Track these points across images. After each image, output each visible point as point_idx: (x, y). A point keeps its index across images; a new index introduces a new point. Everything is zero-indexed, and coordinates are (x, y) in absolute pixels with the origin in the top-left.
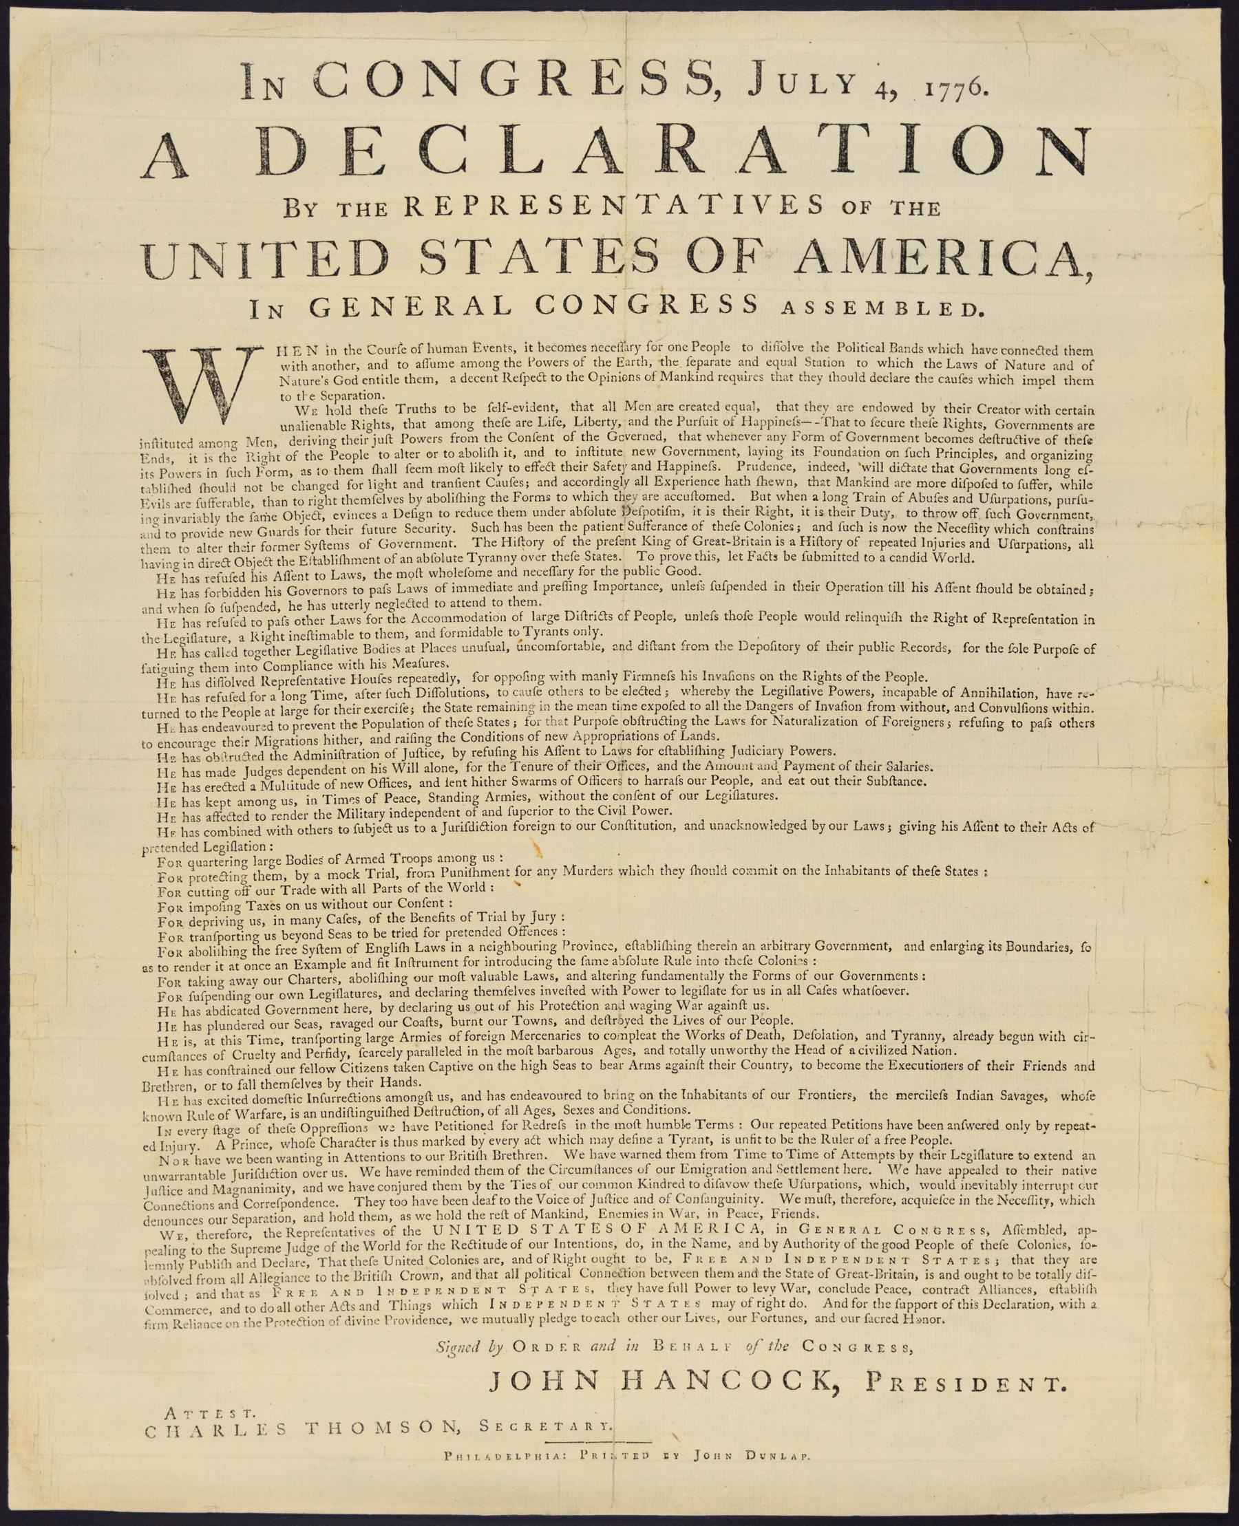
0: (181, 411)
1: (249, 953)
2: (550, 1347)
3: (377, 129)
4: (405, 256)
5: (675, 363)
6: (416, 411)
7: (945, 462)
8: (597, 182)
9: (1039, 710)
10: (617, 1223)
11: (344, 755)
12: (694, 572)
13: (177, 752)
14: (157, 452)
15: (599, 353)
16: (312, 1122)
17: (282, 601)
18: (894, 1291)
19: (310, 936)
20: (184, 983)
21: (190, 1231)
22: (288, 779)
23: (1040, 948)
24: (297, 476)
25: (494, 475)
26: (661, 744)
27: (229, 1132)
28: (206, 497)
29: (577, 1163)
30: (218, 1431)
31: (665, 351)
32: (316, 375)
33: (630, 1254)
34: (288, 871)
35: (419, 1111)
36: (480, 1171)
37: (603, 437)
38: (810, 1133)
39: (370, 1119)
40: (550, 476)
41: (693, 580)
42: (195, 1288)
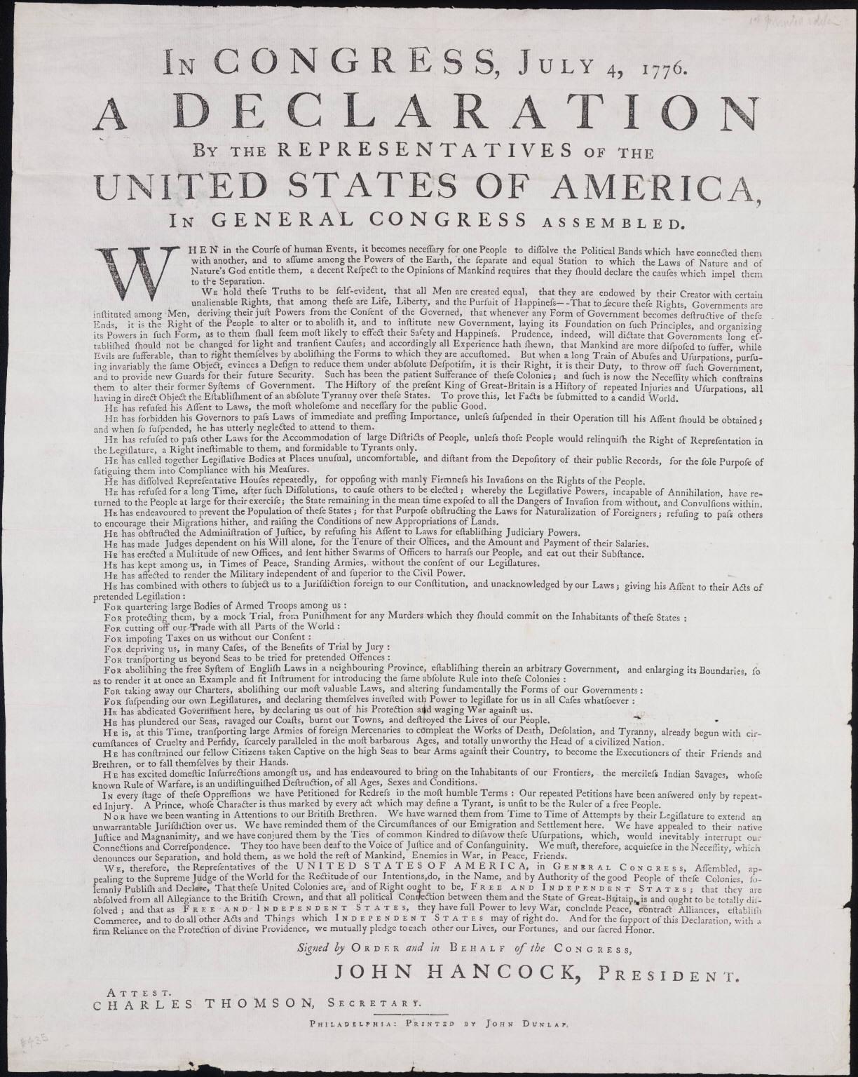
0: (122, 292)
1: (168, 671)
3: (259, 96)
4: (279, 185)
5: (468, 261)
7: (657, 332)
9: (723, 504)
10: (425, 862)
11: (235, 533)
13: (118, 530)
14: (105, 321)
15: (414, 253)
16: (212, 790)
17: (193, 425)
19: (212, 659)
21: (126, 866)
22: (196, 549)
25: (341, 338)
26: (458, 527)
27: (154, 797)
28: (139, 352)
29: (397, 819)
30: (144, 1005)
31: (461, 253)
32: (217, 267)
34: (195, 614)
35: (287, 783)
36: (329, 825)
39: (252, 787)
40: (380, 339)
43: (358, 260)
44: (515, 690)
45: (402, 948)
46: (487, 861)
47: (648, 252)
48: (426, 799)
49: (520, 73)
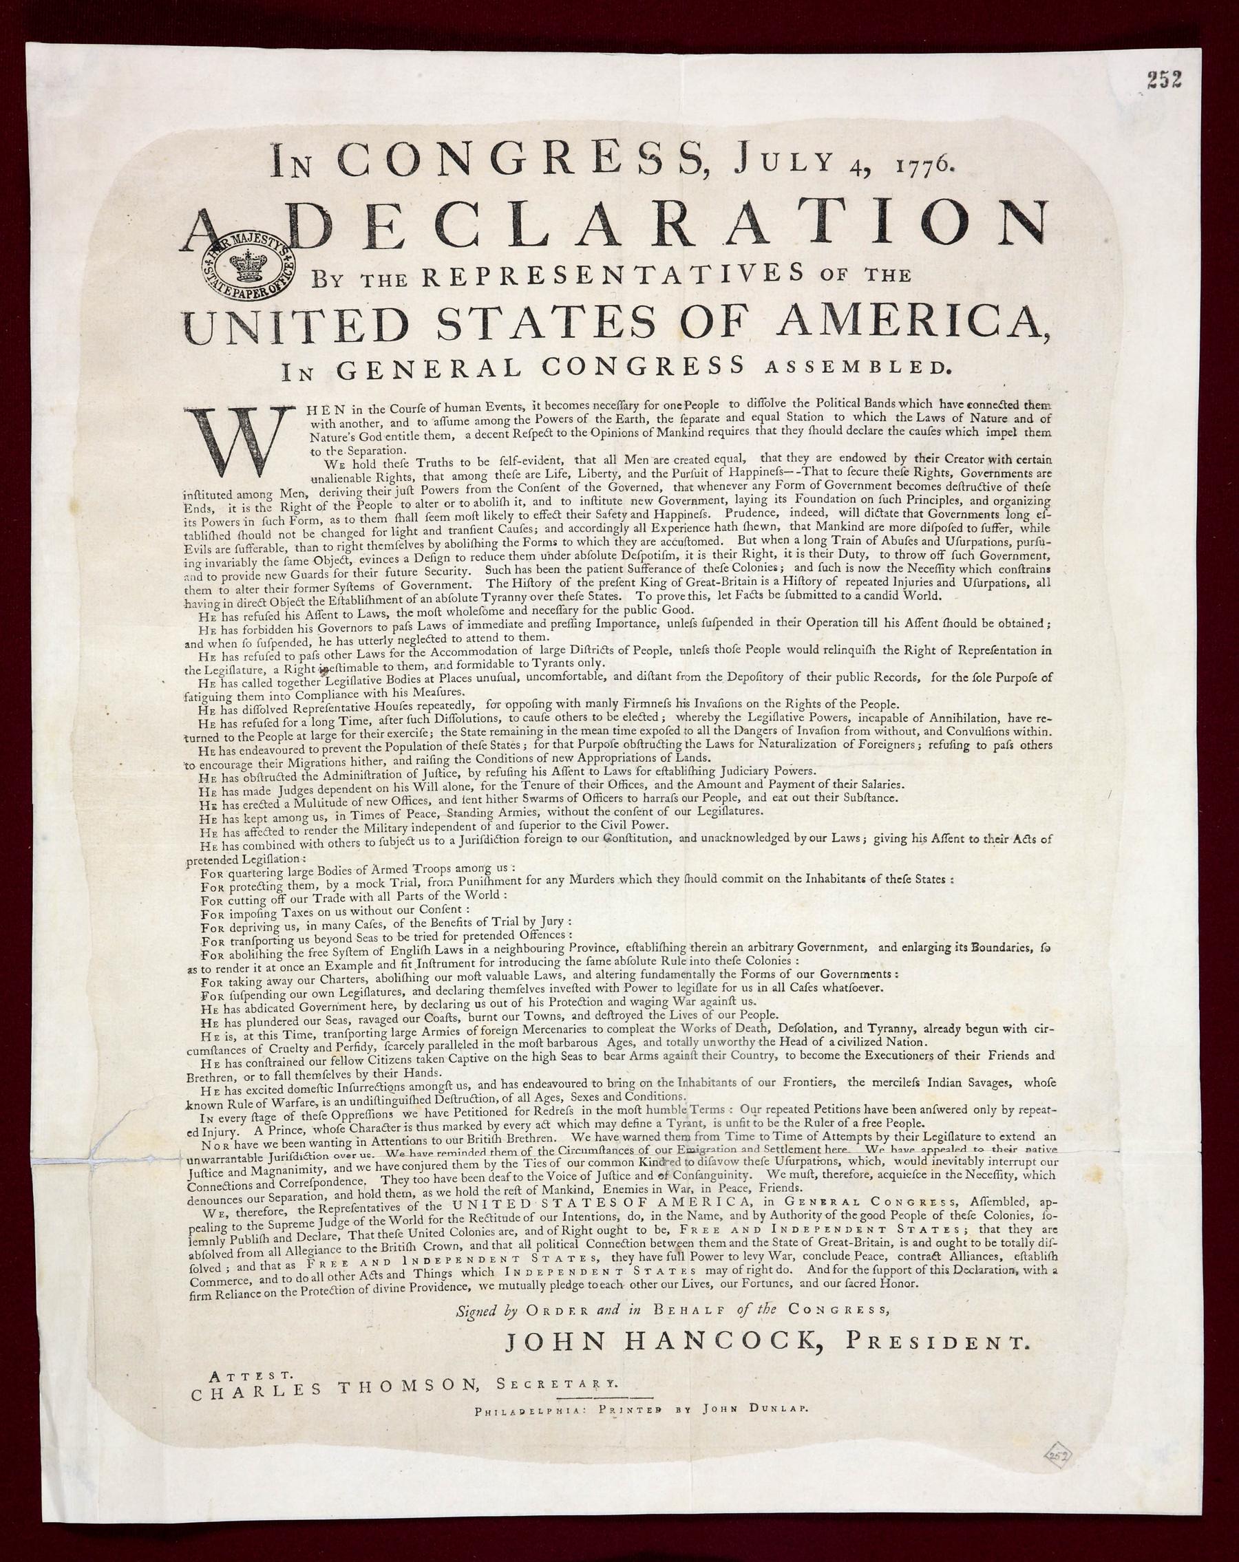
0: (221, 466)
1: (284, 956)
2: (559, 1311)
3: (397, 206)
4: (424, 323)
5: (670, 420)
6: (434, 464)
7: (915, 507)
8: (598, 253)
9: (1001, 732)
10: (620, 1198)
11: (368, 775)
12: (687, 610)
13: (217, 773)
14: (198, 503)
15: (600, 411)
16: (342, 1109)
17: (313, 638)
18: (872, 1258)
19: (342, 939)
20: (225, 983)
21: (230, 1209)
22: (318, 797)
23: (1003, 949)
24: (327, 524)
25: (505, 522)
26: (659, 765)
27: (268, 1119)
28: (244, 543)
29: (583, 1144)
30: (258, 1391)
31: (661, 410)
32: (343, 432)
33: (632, 1226)
34: (320, 882)
35: (440, 1099)
36: (495, 1152)
37: (605, 489)
38: (795, 1117)
39: (395, 1106)
40: (557, 523)
41: (687, 618)
42: (236, 1262)
43: (527, 421)
44: (733, 975)
45: (592, 1310)
46: (699, 1195)
47: (903, 404)
48: (621, 1118)
49: (737, 171)
